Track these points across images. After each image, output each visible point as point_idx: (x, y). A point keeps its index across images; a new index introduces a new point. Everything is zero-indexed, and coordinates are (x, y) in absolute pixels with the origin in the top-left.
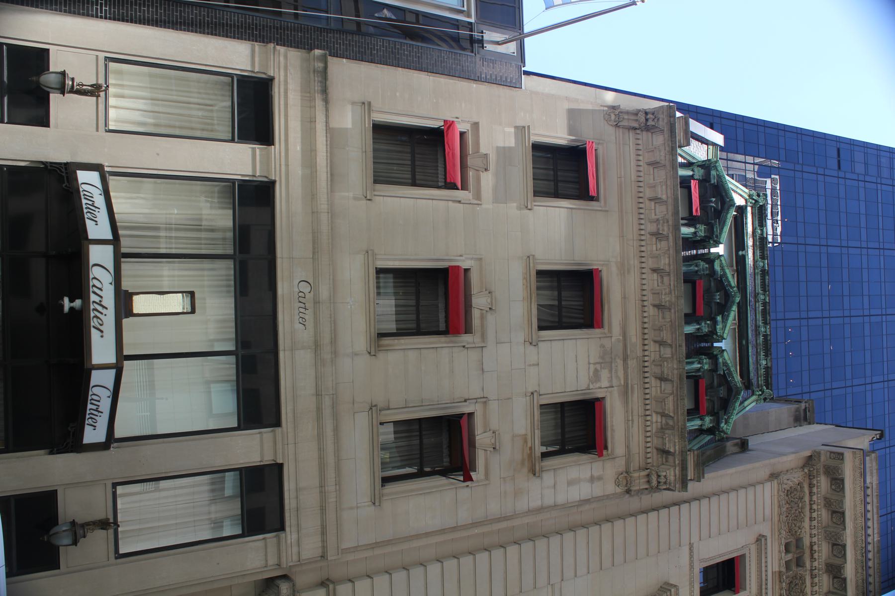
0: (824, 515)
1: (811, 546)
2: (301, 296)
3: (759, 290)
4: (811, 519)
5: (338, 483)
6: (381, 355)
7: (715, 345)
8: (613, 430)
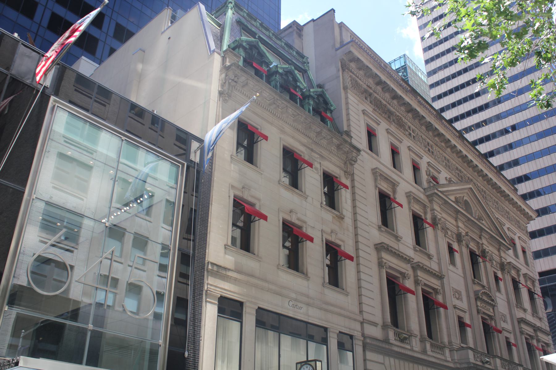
0: (379, 88)
1: (367, 86)
2: (294, 306)
3: (267, 33)
4: (360, 80)
6: (309, 275)
7: (271, 67)
8: (333, 171)
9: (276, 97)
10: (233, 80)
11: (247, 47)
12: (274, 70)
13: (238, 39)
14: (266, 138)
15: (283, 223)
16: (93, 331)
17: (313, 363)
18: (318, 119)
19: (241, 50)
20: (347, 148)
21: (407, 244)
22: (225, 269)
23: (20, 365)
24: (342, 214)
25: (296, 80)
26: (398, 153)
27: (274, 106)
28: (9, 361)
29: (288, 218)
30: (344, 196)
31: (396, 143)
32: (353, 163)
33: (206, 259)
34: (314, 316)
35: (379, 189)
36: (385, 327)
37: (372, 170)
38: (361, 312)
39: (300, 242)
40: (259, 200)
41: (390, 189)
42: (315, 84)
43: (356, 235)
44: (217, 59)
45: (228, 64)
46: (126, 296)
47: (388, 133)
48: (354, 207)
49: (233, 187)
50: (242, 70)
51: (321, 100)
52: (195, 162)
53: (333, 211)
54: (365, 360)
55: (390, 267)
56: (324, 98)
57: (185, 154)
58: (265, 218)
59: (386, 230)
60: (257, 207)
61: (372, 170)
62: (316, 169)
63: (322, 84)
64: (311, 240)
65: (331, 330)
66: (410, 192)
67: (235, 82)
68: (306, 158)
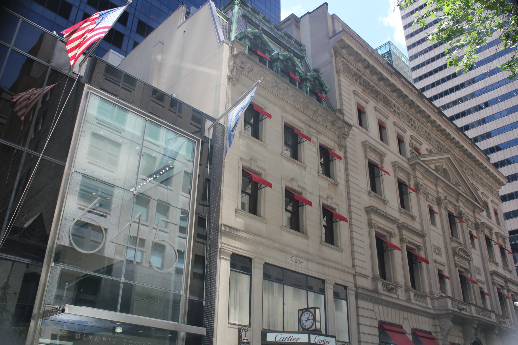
0: (367, 71)
1: (357, 69)
2: (296, 261)
3: (269, 25)
4: (351, 64)
5: (337, 263)
6: (308, 234)
8: (328, 144)
9: (278, 80)
10: (240, 66)
11: (252, 37)
12: (275, 57)
13: (243, 30)
14: (270, 116)
15: (286, 190)
16: (125, 284)
17: (312, 310)
18: (315, 99)
19: (247, 40)
20: (340, 124)
21: (393, 207)
22: (236, 230)
23: (66, 311)
24: (337, 181)
25: (295, 65)
26: (385, 128)
27: (277, 88)
28: (57, 309)
29: (289, 185)
30: (338, 166)
31: (383, 119)
32: (346, 137)
33: (220, 222)
34: (312, 270)
35: (369, 159)
36: (374, 279)
37: (362, 143)
38: (354, 266)
39: (300, 206)
40: (265, 170)
41: (378, 159)
42: (311, 68)
43: (349, 199)
44: (226, 48)
45: (236, 52)
46: (152, 254)
47: (376, 110)
48: (347, 175)
49: (241, 159)
50: (248, 57)
51: (317, 82)
52: (209, 138)
53: (329, 179)
54: (357, 307)
55: (379, 227)
56: (319, 81)
57: (200, 131)
58: (270, 185)
59: (375, 195)
60: (263, 177)
61: (362, 143)
62: (314, 143)
63: (317, 68)
64: (310, 204)
65: (328, 282)
66: (396, 162)
67: (242, 68)
68: (305, 133)
